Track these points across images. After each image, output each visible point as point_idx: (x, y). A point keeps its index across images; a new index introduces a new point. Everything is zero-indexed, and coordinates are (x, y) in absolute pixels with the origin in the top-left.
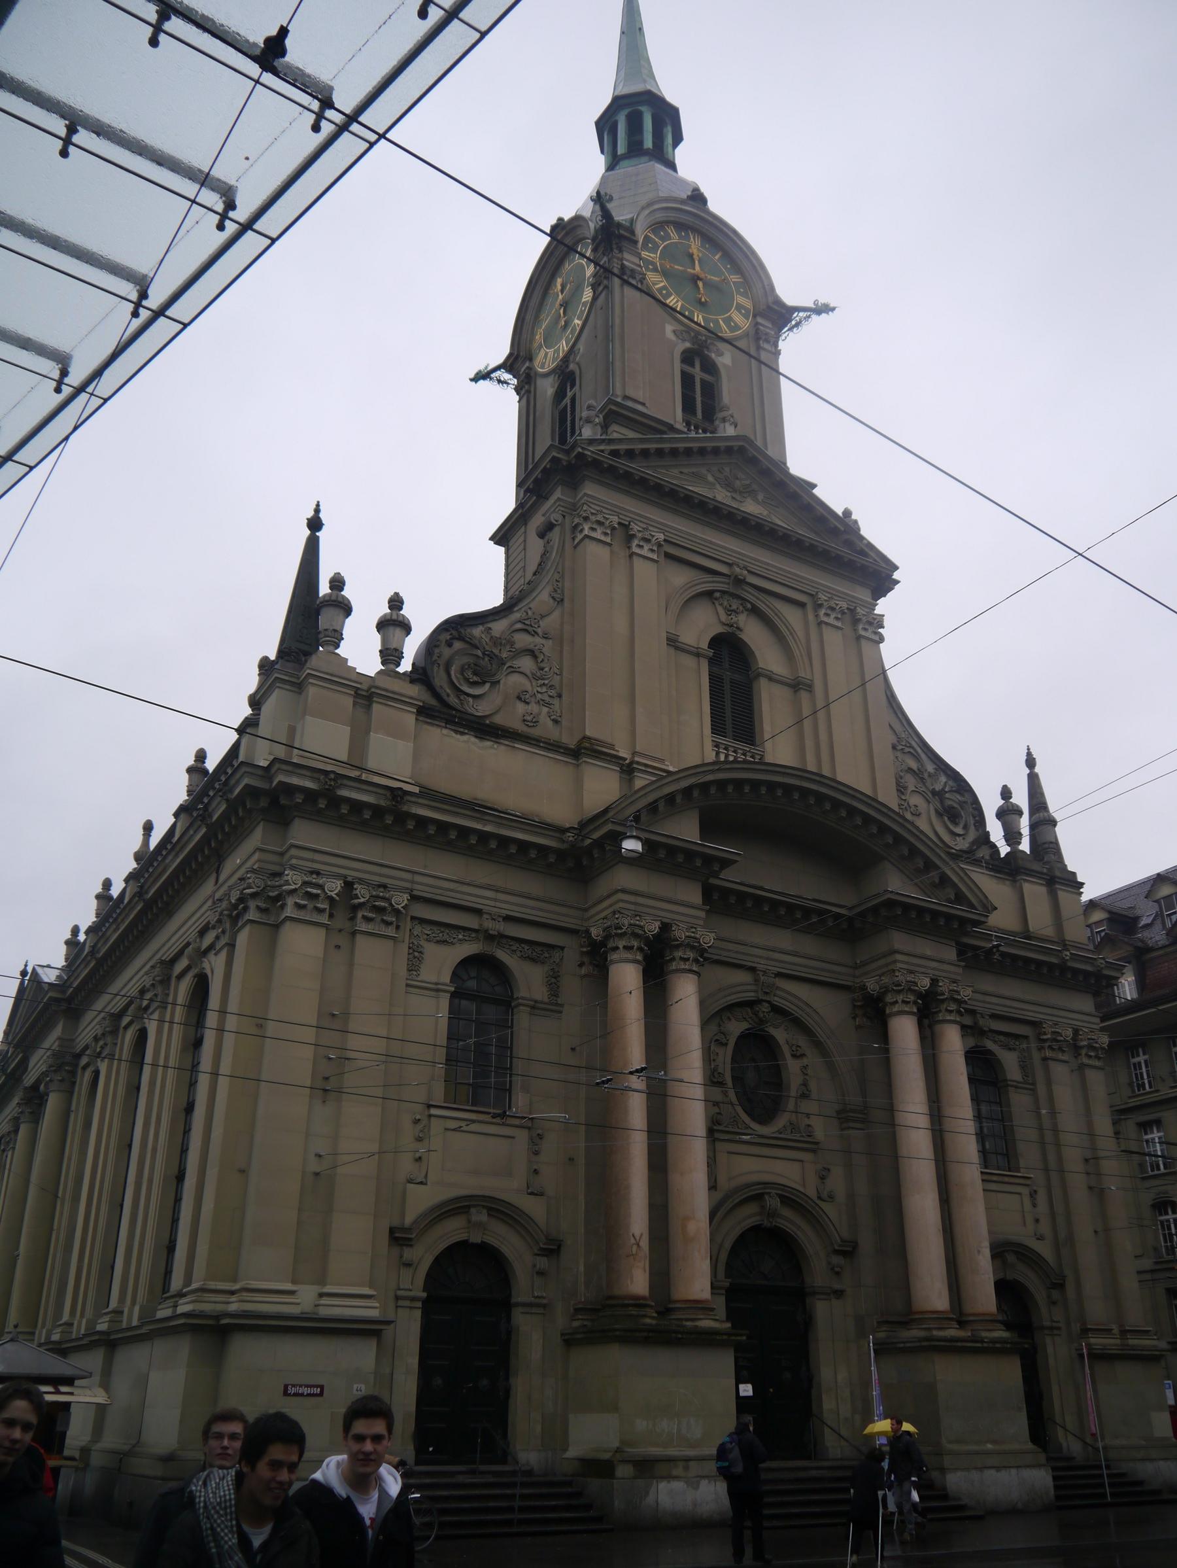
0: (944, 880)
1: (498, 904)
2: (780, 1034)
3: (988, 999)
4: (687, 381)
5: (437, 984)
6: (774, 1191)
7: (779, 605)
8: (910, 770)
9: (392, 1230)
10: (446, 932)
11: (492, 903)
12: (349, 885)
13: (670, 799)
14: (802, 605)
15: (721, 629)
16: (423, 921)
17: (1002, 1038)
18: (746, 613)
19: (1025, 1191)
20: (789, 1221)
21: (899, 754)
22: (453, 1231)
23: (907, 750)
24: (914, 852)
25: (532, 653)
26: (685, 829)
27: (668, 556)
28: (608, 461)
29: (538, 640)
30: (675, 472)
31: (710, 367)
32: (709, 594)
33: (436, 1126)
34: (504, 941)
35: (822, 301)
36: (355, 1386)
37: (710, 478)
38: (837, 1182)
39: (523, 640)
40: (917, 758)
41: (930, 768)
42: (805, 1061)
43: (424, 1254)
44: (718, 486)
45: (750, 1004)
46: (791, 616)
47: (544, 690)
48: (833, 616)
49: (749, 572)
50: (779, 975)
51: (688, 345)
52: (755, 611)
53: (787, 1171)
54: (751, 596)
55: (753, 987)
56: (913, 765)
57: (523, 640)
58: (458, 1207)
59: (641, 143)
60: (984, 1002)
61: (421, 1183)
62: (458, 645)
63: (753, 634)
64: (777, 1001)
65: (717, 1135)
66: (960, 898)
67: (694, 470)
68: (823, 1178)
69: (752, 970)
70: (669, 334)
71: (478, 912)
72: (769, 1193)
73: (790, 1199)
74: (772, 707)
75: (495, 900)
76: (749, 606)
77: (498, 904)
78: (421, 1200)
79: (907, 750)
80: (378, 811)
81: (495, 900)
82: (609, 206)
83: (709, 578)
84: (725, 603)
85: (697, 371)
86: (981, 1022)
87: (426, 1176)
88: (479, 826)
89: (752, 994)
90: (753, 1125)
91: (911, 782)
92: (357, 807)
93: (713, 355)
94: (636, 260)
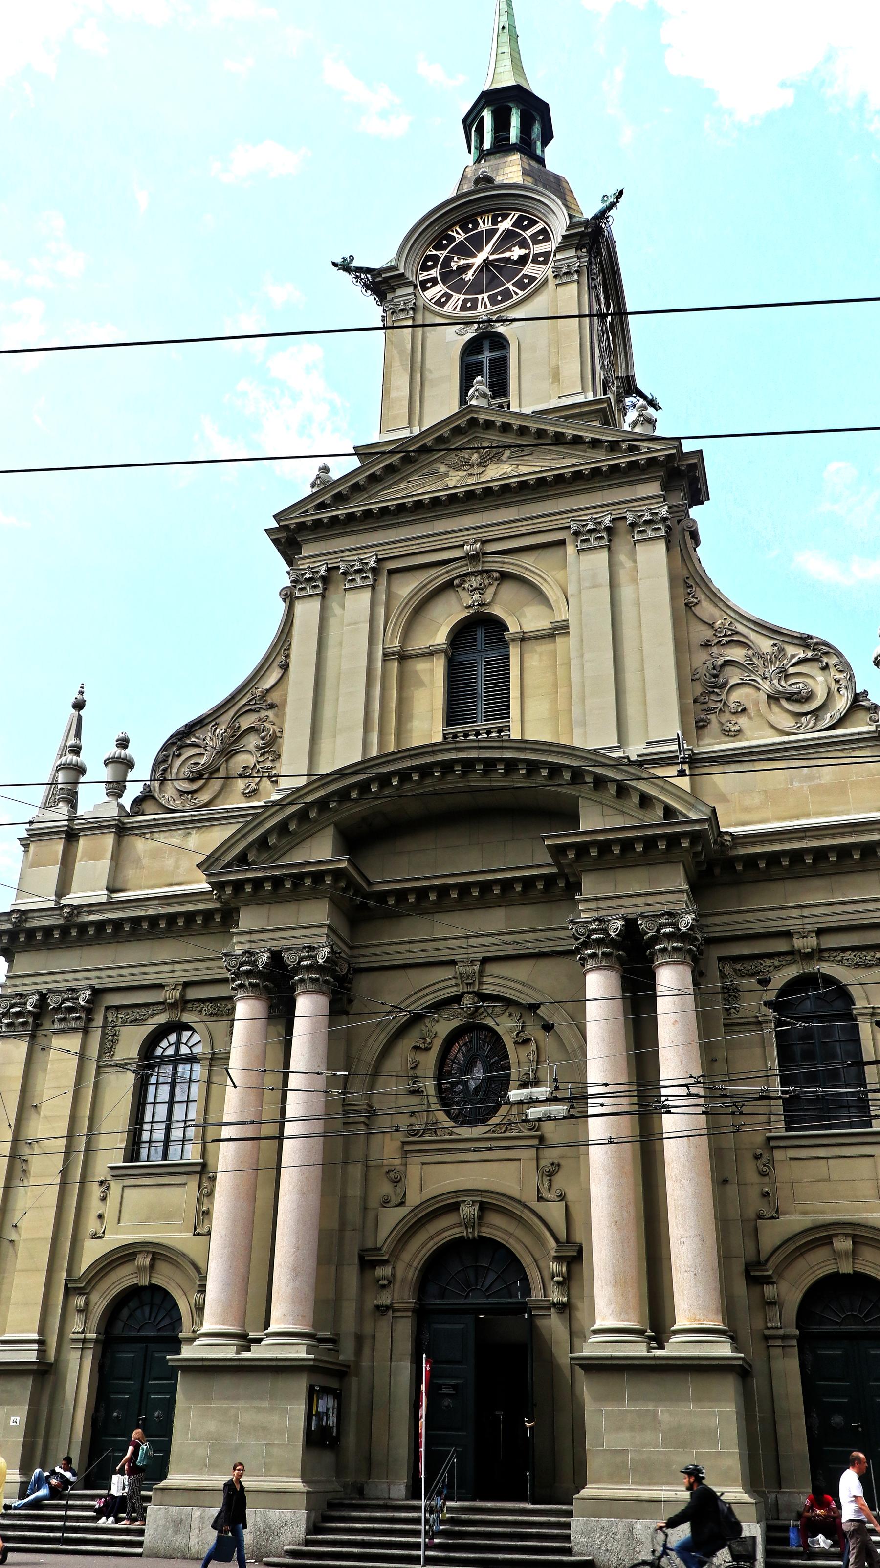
0: (646, 801)
1: (176, 975)
2: (504, 1025)
3: (806, 912)
5: (124, 1059)
6: (469, 1199)
10: (135, 1013)
11: (170, 975)
12: (43, 997)
13: (282, 828)
14: (562, 543)
15: (466, 614)
16: (118, 1008)
17: (848, 955)
18: (496, 583)
20: (498, 1228)
21: (715, 650)
22: (124, 1278)
23: (727, 639)
24: (600, 782)
25: (251, 730)
26: (320, 850)
27: (391, 572)
29: (263, 714)
30: (404, 484)
31: (500, 343)
32: (449, 586)
33: (116, 1187)
34: (190, 1005)
35: (611, 191)
36: (12, 1418)
37: (443, 469)
41: (765, 645)
42: (533, 1046)
43: (100, 1301)
44: (452, 473)
45: (457, 999)
46: (528, 565)
47: (266, 756)
48: (592, 540)
49: (484, 542)
50: (485, 961)
54: (496, 564)
55: (453, 982)
57: (246, 723)
58: (124, 1255)
60: (803, 917)
61: (100, 1237)
64: (486, 989)
65: (407, 1148)
66: (669, 812)
67: (426, 471)
68: (550, 1175)
69: (453, 963)
71: (160, 986)
72: (465, 1201)
73: (489, 1204)
74: (528, 670)
75: (173, 971)
76: (496, 575)
77: (176, 975)
78: (92, 1252)
79: (727, 639)
80: (65, 930)
81: (173, 971)
82: (355, 264)
83: (442, 569)
84: (466, 586)
86: (798, 943)
87: (104, 1232)
88: (142, 913)
89: (455, 989)
92: (48, 931)
94: (411, 290)
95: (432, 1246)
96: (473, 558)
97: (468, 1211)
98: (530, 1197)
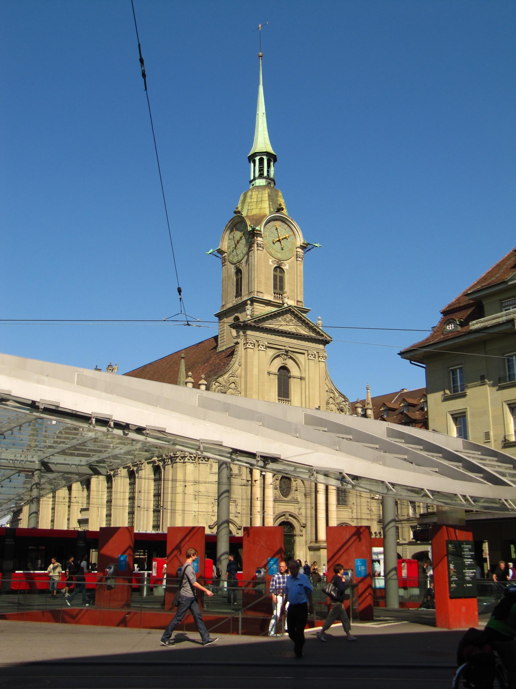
4: (275, 277)
7: (297, 355)
8: (331, 397)
9: (209, 526)
14: (304, 354)
19: (350, 510)
28: (253, 324)
31: (282, 271)
38: (303, 511)
39: (232, 379)
40: (334, 393)
41: (337, 395)
51: (276, 265)
52: (291, 358)
53: (291, 508)
56: (332, 395)
59: (263, 174)
62: (217, 384)
63: (290, 364)
70: (271, 263)
85: (278, 274)
90: (284, 498)
91: (331, 401)
93: (283, 267)
95: (279, 522)
96: (287, 351)
97: (287, 516)
98: (297, 514)
